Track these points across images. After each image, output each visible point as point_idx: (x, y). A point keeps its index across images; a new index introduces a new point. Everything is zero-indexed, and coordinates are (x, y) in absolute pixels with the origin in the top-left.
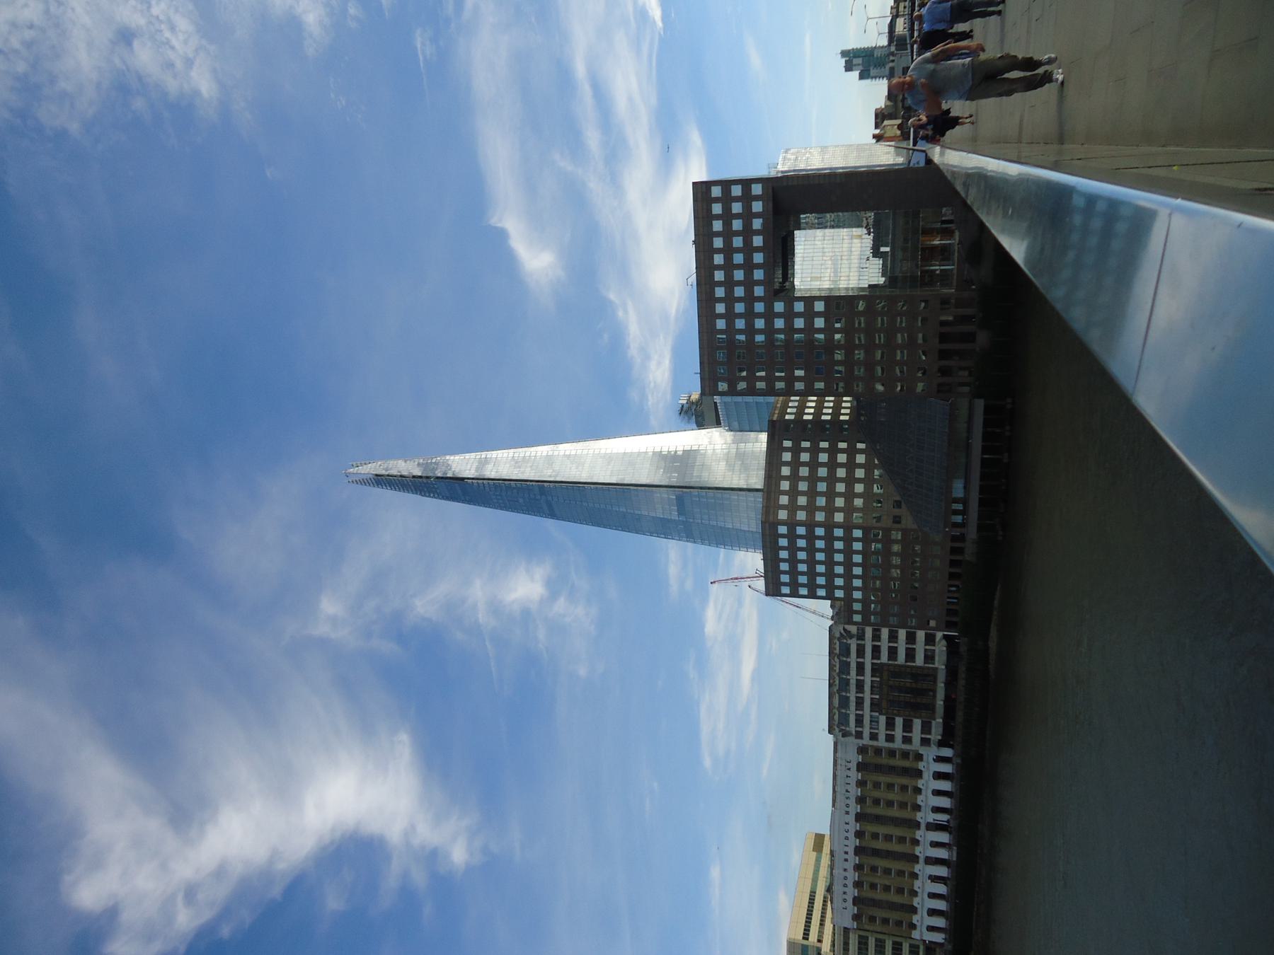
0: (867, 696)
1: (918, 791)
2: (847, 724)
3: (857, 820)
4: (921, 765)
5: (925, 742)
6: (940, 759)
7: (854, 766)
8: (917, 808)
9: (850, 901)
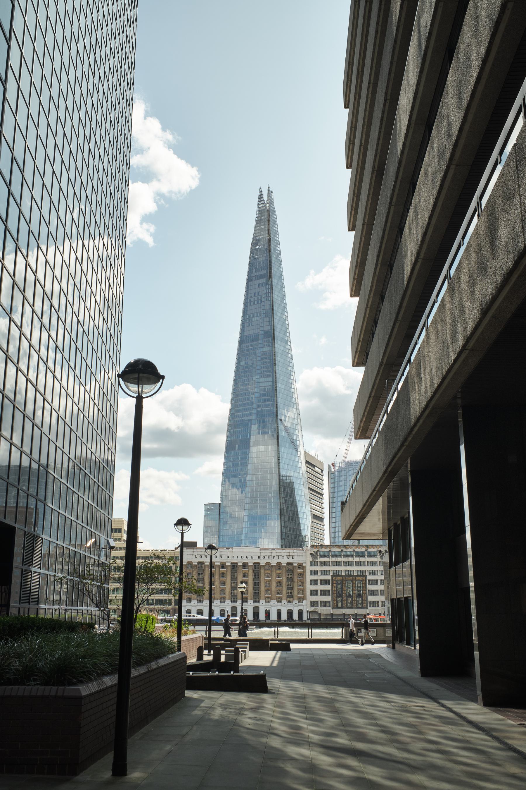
0: (342, 568)
1: (279, 600)
2: (321, 556)
3: (254, 563)
4: (296, 602)
5: (314, 604)
6: (300, 613)
7: (290, 561)
8: (268, 600)
9: (201, 560)
